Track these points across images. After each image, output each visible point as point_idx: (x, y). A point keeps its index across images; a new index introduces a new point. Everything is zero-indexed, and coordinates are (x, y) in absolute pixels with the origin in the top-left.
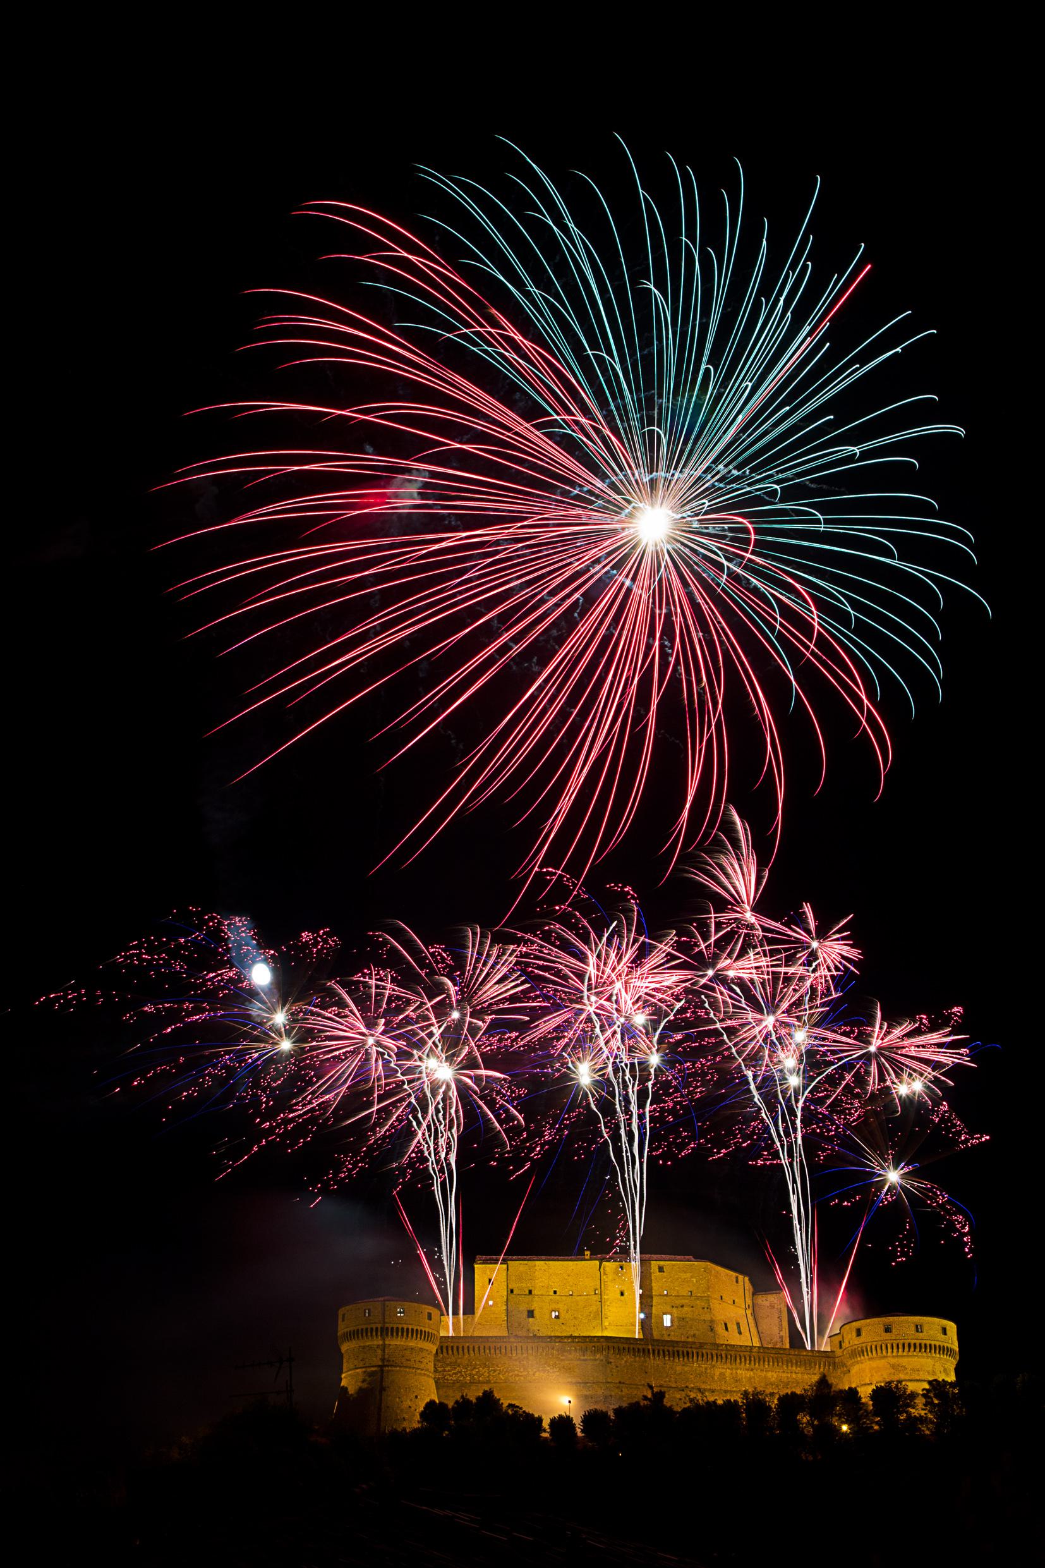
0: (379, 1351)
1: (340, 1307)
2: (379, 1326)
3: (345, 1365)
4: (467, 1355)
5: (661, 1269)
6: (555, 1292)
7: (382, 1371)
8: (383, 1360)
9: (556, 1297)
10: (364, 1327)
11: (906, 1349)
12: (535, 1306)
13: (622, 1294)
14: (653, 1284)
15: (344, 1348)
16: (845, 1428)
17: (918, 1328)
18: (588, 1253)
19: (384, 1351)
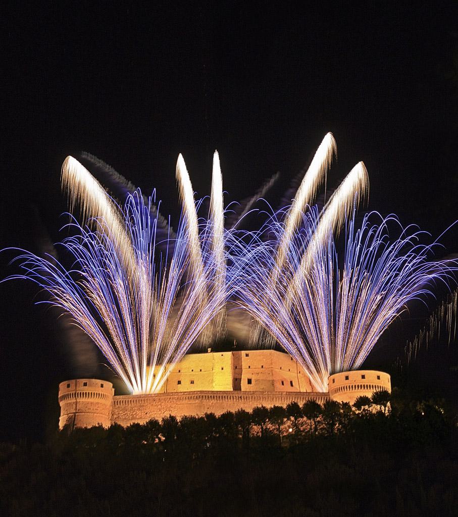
0: (74, 406)
1: (61, 382)
2: (74, 392)
3: (62, 411)
4: (130, 405)
5: (247, 355)
6: (192, 370)
7: (75, 416)
8: (76, 409)
9: (193, 373)
10: (67, 393)
11: (357, 388)
12: (182, 379)
13: (222, 369)
14: (243, 363)
15: (62, 404)
16: (423, 414)
17: (363, 377)
18: (209, 350)
19: (76, 405)
